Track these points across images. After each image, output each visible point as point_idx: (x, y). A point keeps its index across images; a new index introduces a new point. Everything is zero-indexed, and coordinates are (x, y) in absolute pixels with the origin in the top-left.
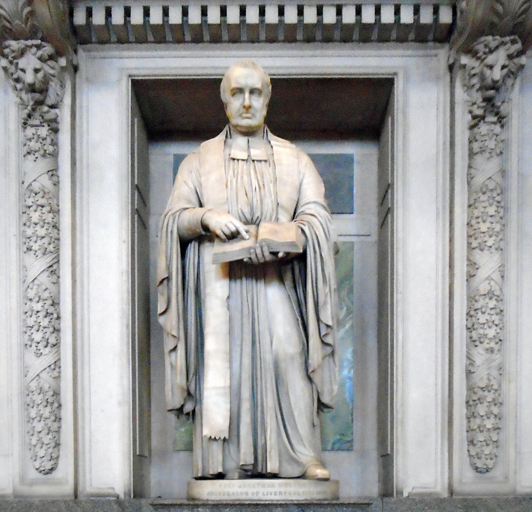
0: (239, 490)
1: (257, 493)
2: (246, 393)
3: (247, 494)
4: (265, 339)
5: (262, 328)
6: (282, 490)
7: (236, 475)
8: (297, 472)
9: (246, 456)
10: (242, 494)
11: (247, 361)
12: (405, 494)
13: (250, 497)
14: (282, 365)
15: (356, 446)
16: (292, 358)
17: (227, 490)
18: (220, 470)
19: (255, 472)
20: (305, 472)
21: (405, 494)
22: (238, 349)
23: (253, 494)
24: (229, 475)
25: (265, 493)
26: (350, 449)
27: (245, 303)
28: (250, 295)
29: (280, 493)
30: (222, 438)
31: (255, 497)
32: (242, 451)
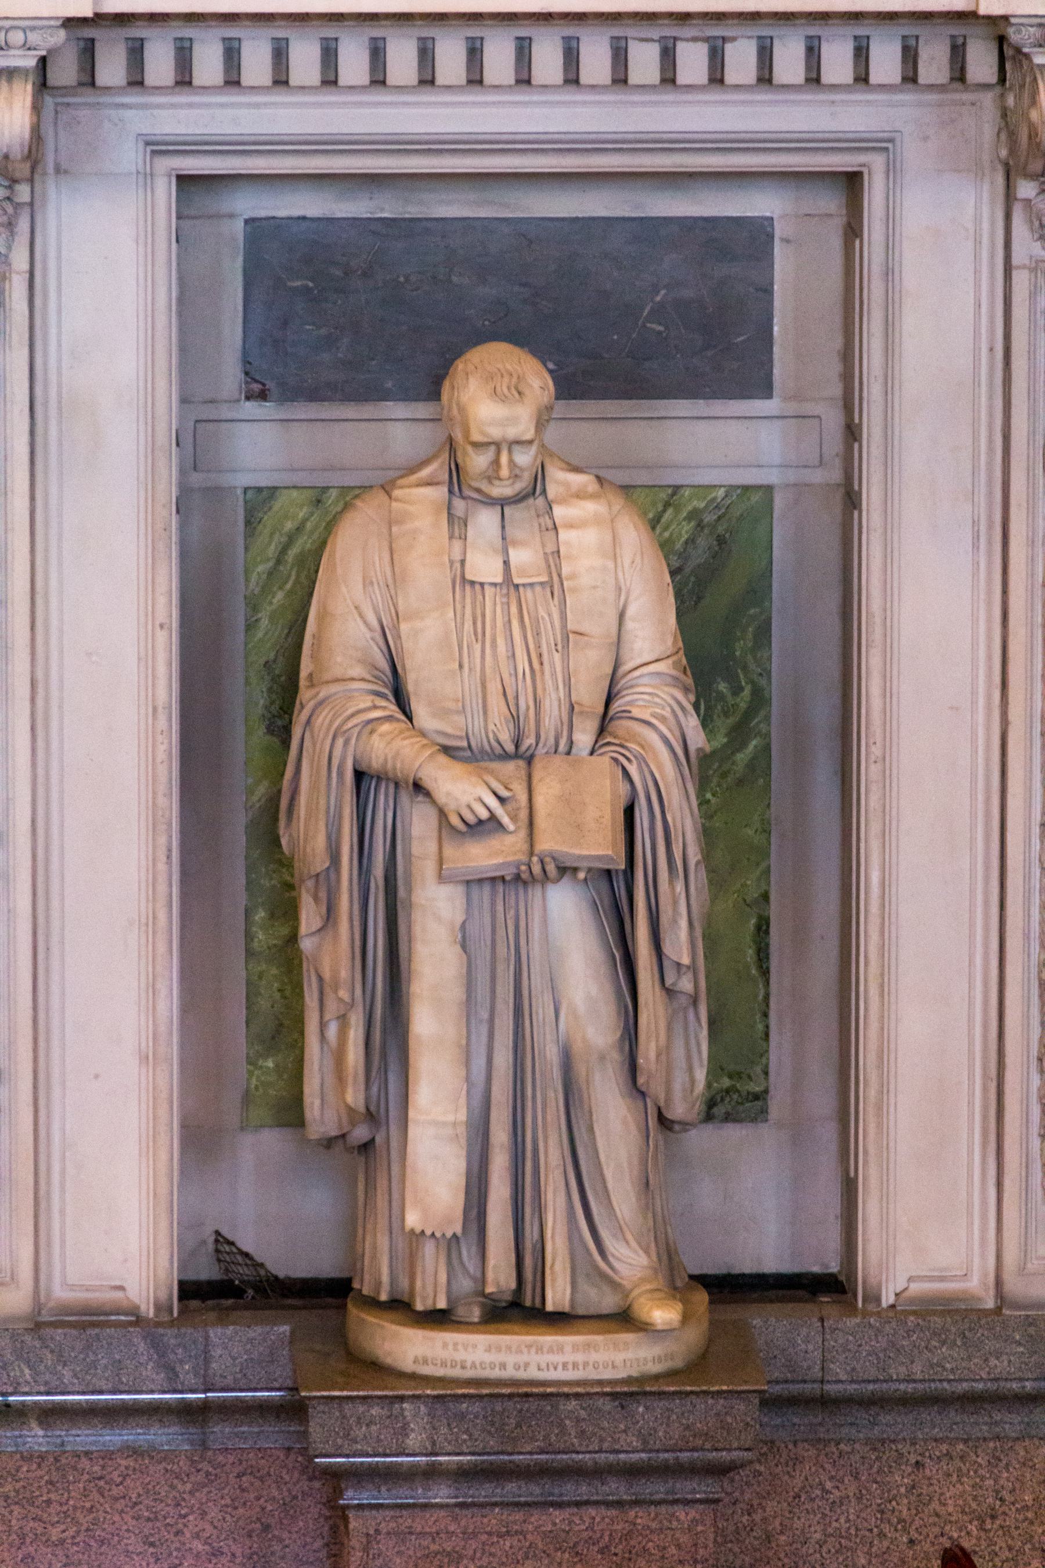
0: (488, 1358)
1: (527, 1365)
2: (500, 1135)
3: (503, 1366)
4: (542, 1008)
5: (536, 980)
6: (580, 1357)
7: (476, 1314)
8: (609, 1302)
9: (500, 1276)
10: (492, 1365)
11: (503, 1059)
12: (888, 1298)
13: (510, 1373)
14: (580, 1069)
15: (778, 1105)
16: (602, 1058)
17: (461, 1355)
18: (442, 1304)
19: (518, 1309)
20: (630, 1306)
21: (888, 1298)
22: (484, 1030)
23: (517, 1367)
24: (461, 1312)
25: (544, 1365)
26: (760, 1115)
27: (501, 932)
28: (511, 913)
29: (575, 1366)
30: (449, 1235)
31: (522, 1375)
32: (492, 1262)
